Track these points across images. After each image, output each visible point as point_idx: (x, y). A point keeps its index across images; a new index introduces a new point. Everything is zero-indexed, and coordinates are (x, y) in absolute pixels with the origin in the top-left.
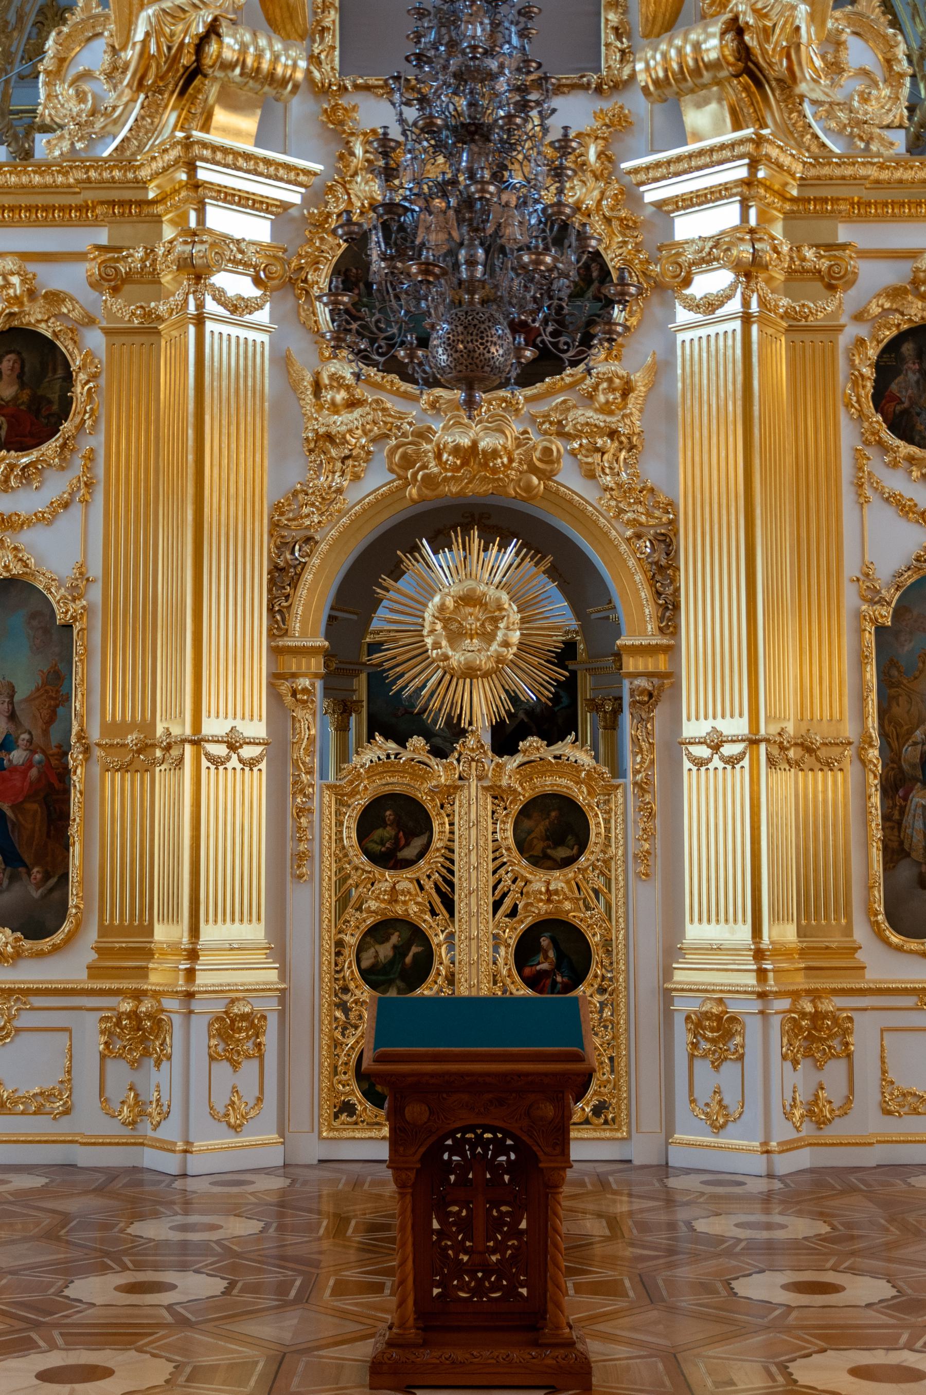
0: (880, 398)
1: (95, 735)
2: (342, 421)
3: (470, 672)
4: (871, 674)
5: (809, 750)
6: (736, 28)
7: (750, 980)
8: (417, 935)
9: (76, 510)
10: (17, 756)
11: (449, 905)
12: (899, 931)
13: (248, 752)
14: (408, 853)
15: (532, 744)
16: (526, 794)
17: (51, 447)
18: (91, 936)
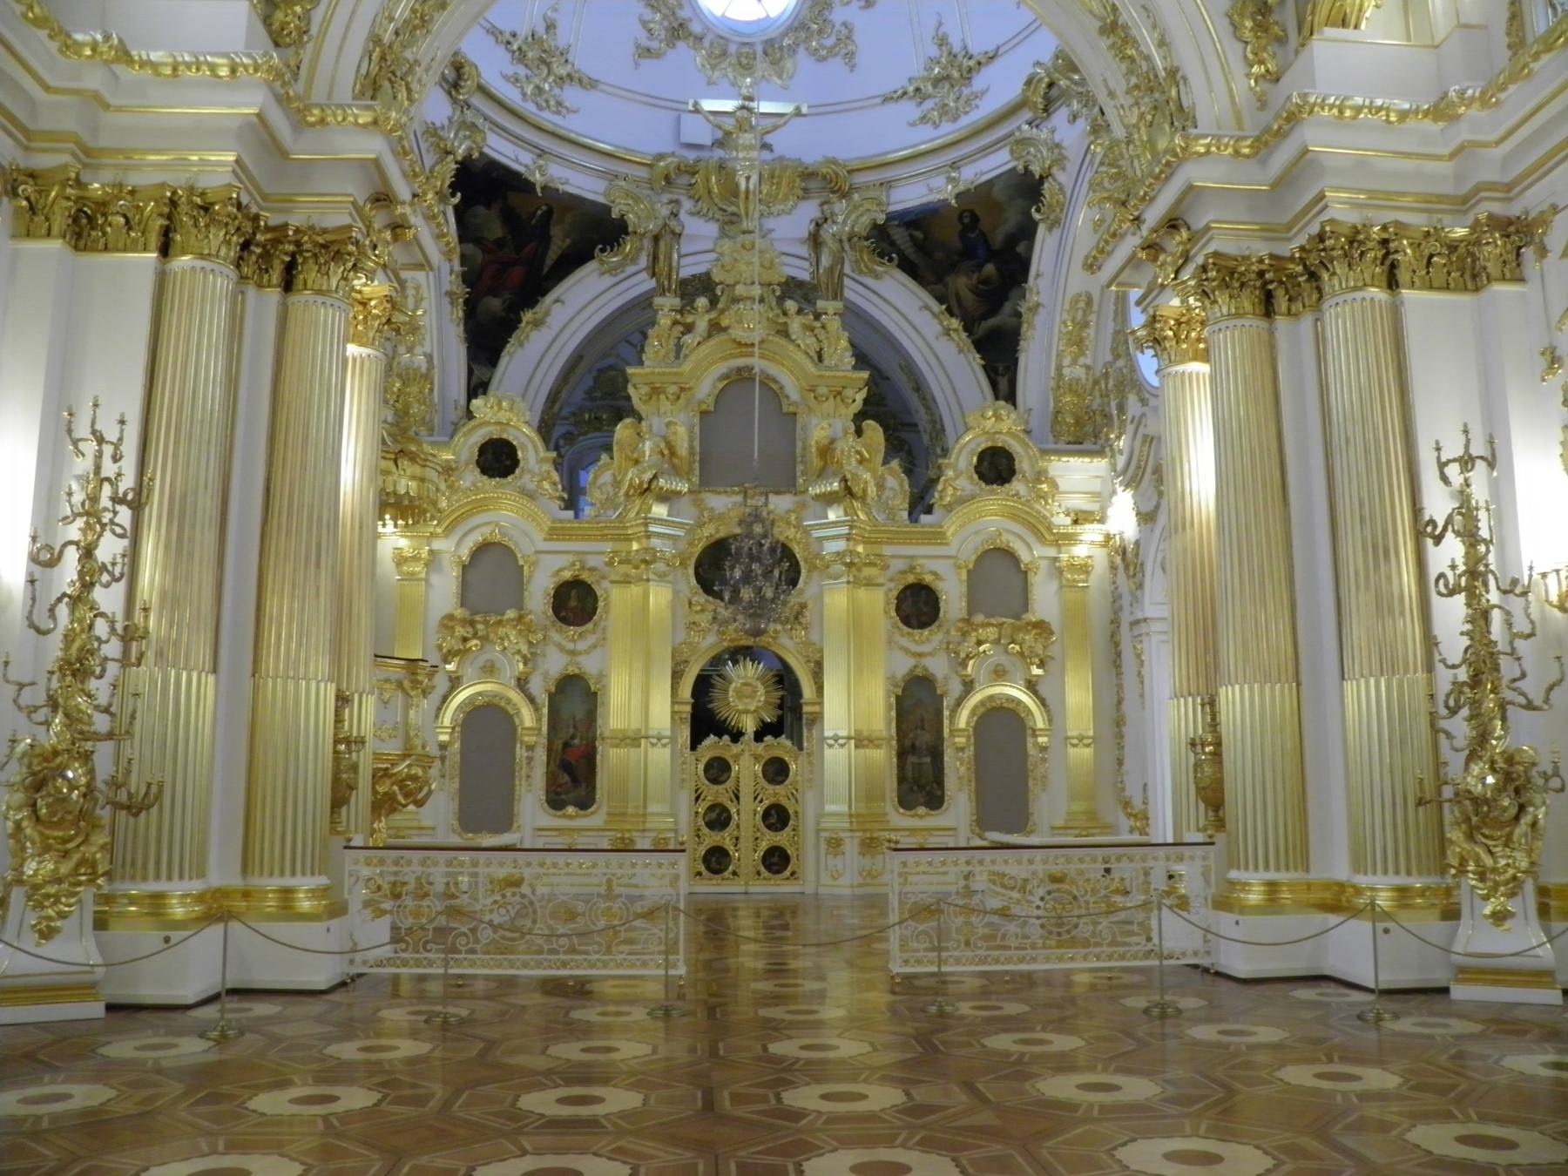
0: (898, 610)
1: (606, 734)
2: (697, 618)
3: (746, 712)
4: (893, 714)
5: (871, 741)
6: (845, 480)
7: (847, 825)
8: (725, 810)
9: (599, 649)
10: (576, 742)
11: (737, 798)
12: (902, 807)
13: (664, 741)
14: (722, 779)
15: (768, 739)
16: (767, 756)
17: (590, 626)
18: (604, 809)
